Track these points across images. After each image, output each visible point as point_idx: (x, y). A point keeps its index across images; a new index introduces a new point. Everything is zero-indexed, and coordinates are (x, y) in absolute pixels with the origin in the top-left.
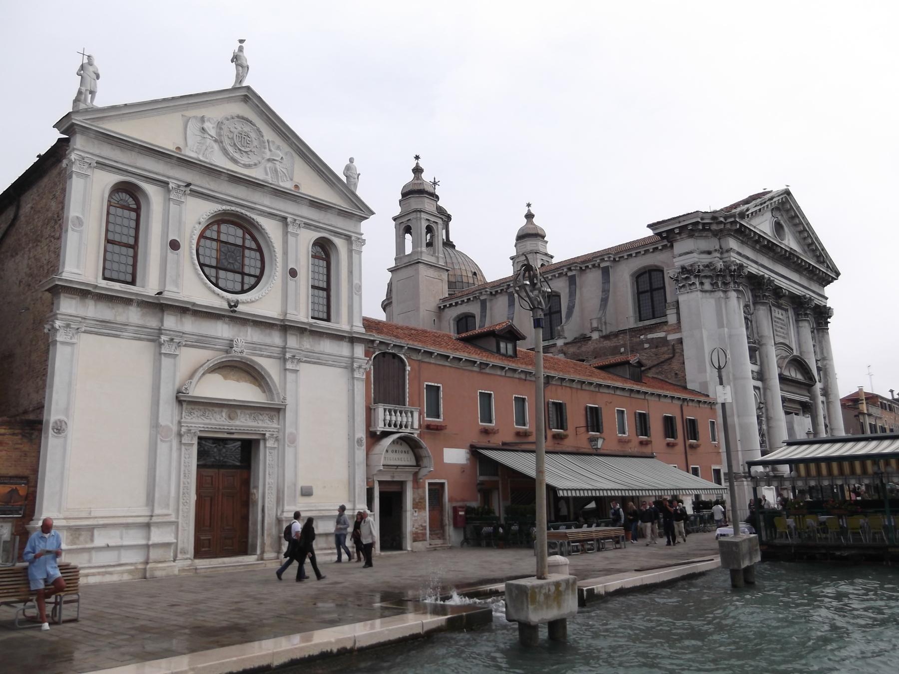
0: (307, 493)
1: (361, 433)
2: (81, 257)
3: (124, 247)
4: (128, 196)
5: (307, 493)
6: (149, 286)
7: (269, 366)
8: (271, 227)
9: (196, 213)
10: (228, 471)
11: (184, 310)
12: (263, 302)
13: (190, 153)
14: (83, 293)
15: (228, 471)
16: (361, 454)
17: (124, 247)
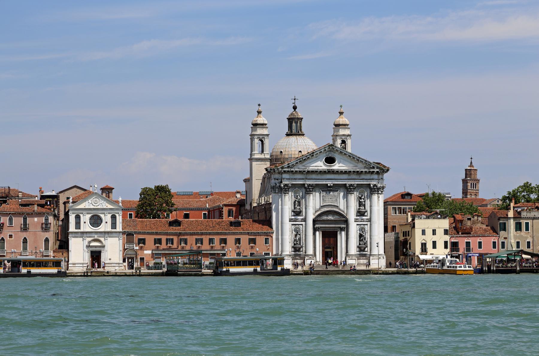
0: (110, 259)
1: (121, 249)
2: (72, 228)
3: (78, 225)
4: (78, 217)
5: (110, 259)
6: (82, 230)
7: (102, 239)
8: (102, 216)
9: (88, 216)
10: (96, 256)
11: (87, 232)
12: (102, 228)
13: (87, 207)
14: (72, 233)
15: (96, 256)
16: (121, 253)
17: (78, 225)
